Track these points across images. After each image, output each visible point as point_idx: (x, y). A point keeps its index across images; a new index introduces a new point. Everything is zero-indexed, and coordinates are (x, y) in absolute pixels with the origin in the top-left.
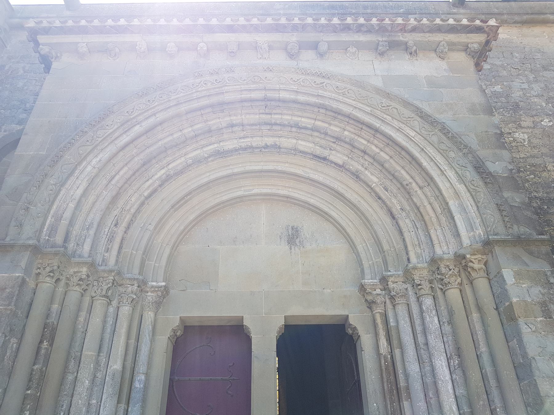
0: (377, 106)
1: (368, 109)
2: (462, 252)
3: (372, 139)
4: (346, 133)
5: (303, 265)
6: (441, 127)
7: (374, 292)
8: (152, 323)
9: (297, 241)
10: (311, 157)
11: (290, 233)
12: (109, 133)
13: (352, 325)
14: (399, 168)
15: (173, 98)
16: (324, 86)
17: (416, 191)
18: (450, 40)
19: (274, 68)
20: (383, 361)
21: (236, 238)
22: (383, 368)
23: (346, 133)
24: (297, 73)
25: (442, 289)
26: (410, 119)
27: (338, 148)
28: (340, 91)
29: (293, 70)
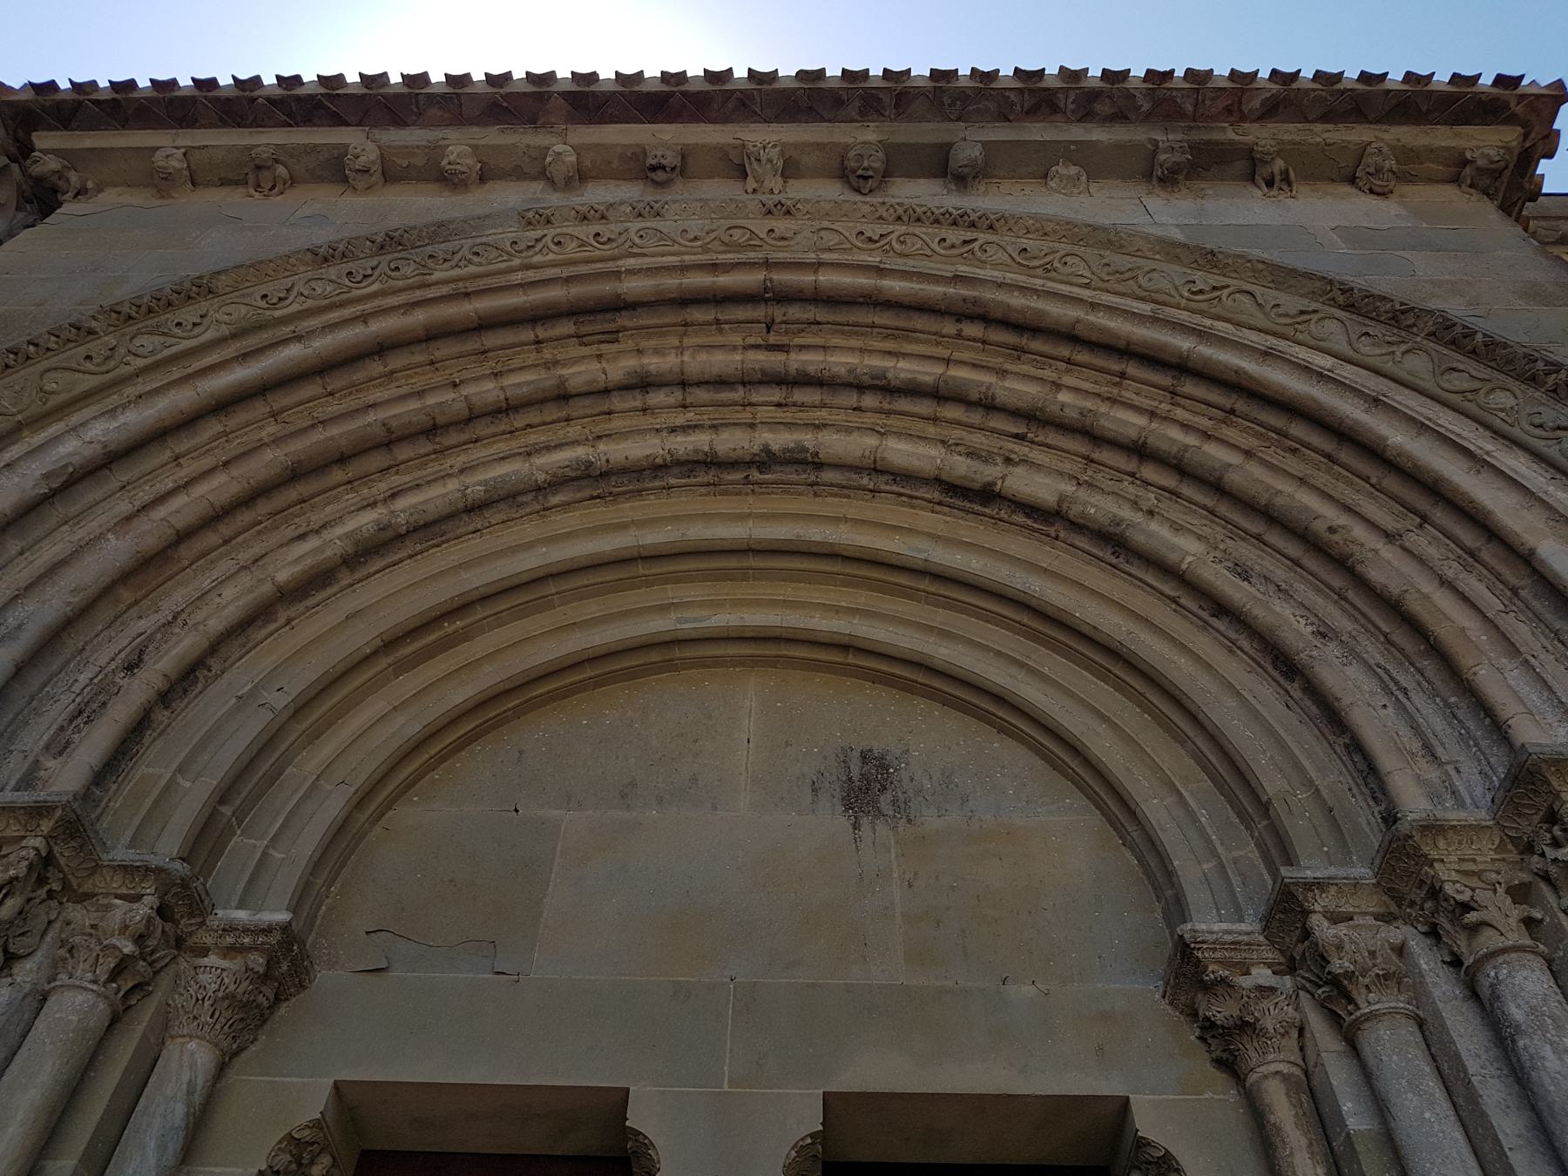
0: (1173, 292)
3: (1165, 407)
5: (910, 886)
7: (1245, 982)
8: (190, 1093)
9: (884, 801)
10: (936, 495)
11: (855, 774)
12: (174, 349)
13: (1148, 1144)
15: (437, 276)
16: (976, 249)
18: (1399, 140)
19: (799, 206)
21: (633, 784)
23: (1064, 397)
24: (881, 218)
26: (1308, 317)
27: (1036, 455)
28: (1036, 263)
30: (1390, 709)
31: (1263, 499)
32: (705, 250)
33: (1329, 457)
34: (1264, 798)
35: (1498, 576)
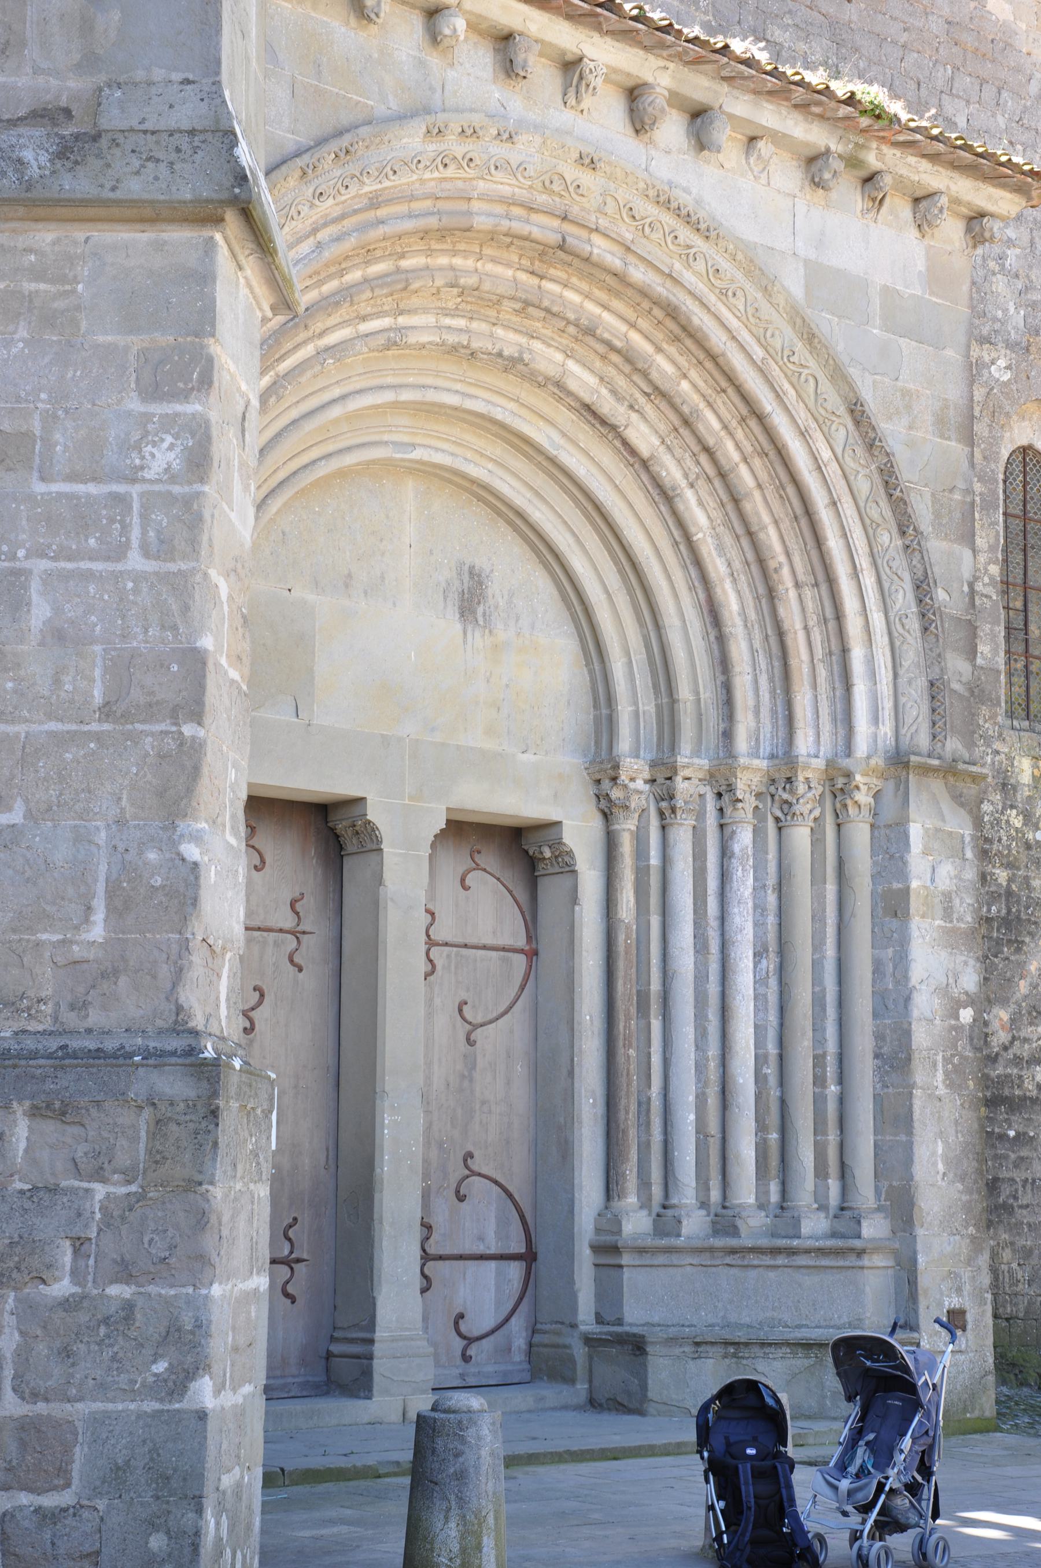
1: (758, 353)
2: (845, 763)
3: (734, 423)
4: (685, 385)
5: (488, 681)
6: (885, 464)
9: (480, 610)
10: (577, 405)
11: (466, 585)
13: (565, 844)
14: (766, 519)
17: (787, 590)
25: (777, 820)
26: (834, 419)
27: (649, 409)
30: (749, 677)
31: (754, 528)
33: (796, 518)
34: (675, 696)
35: (829, 641)
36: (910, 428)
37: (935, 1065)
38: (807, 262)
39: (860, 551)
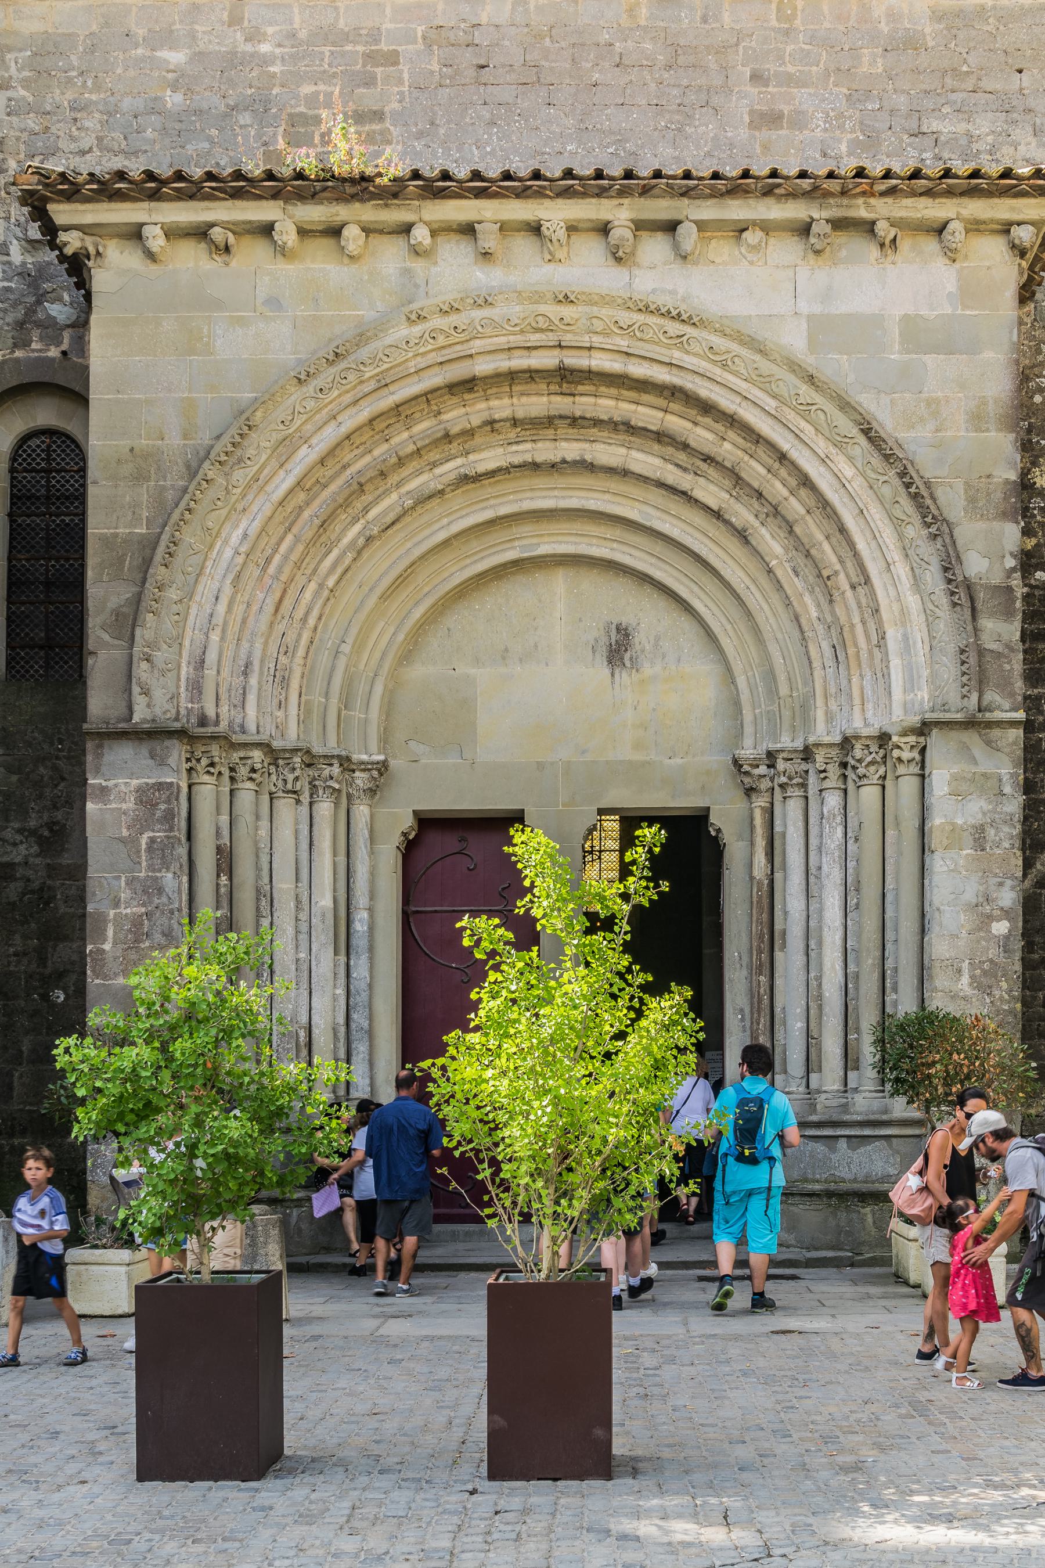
1: (771, 404)
15: (367, 375)
20: (755, 890)
22: (755, 900)
23: (727, 445)
29: (620, 301)
32: (522, 332)
36: (937, 431)
37: (959, 971)
38: (810, 318)
39: (892, 547)
